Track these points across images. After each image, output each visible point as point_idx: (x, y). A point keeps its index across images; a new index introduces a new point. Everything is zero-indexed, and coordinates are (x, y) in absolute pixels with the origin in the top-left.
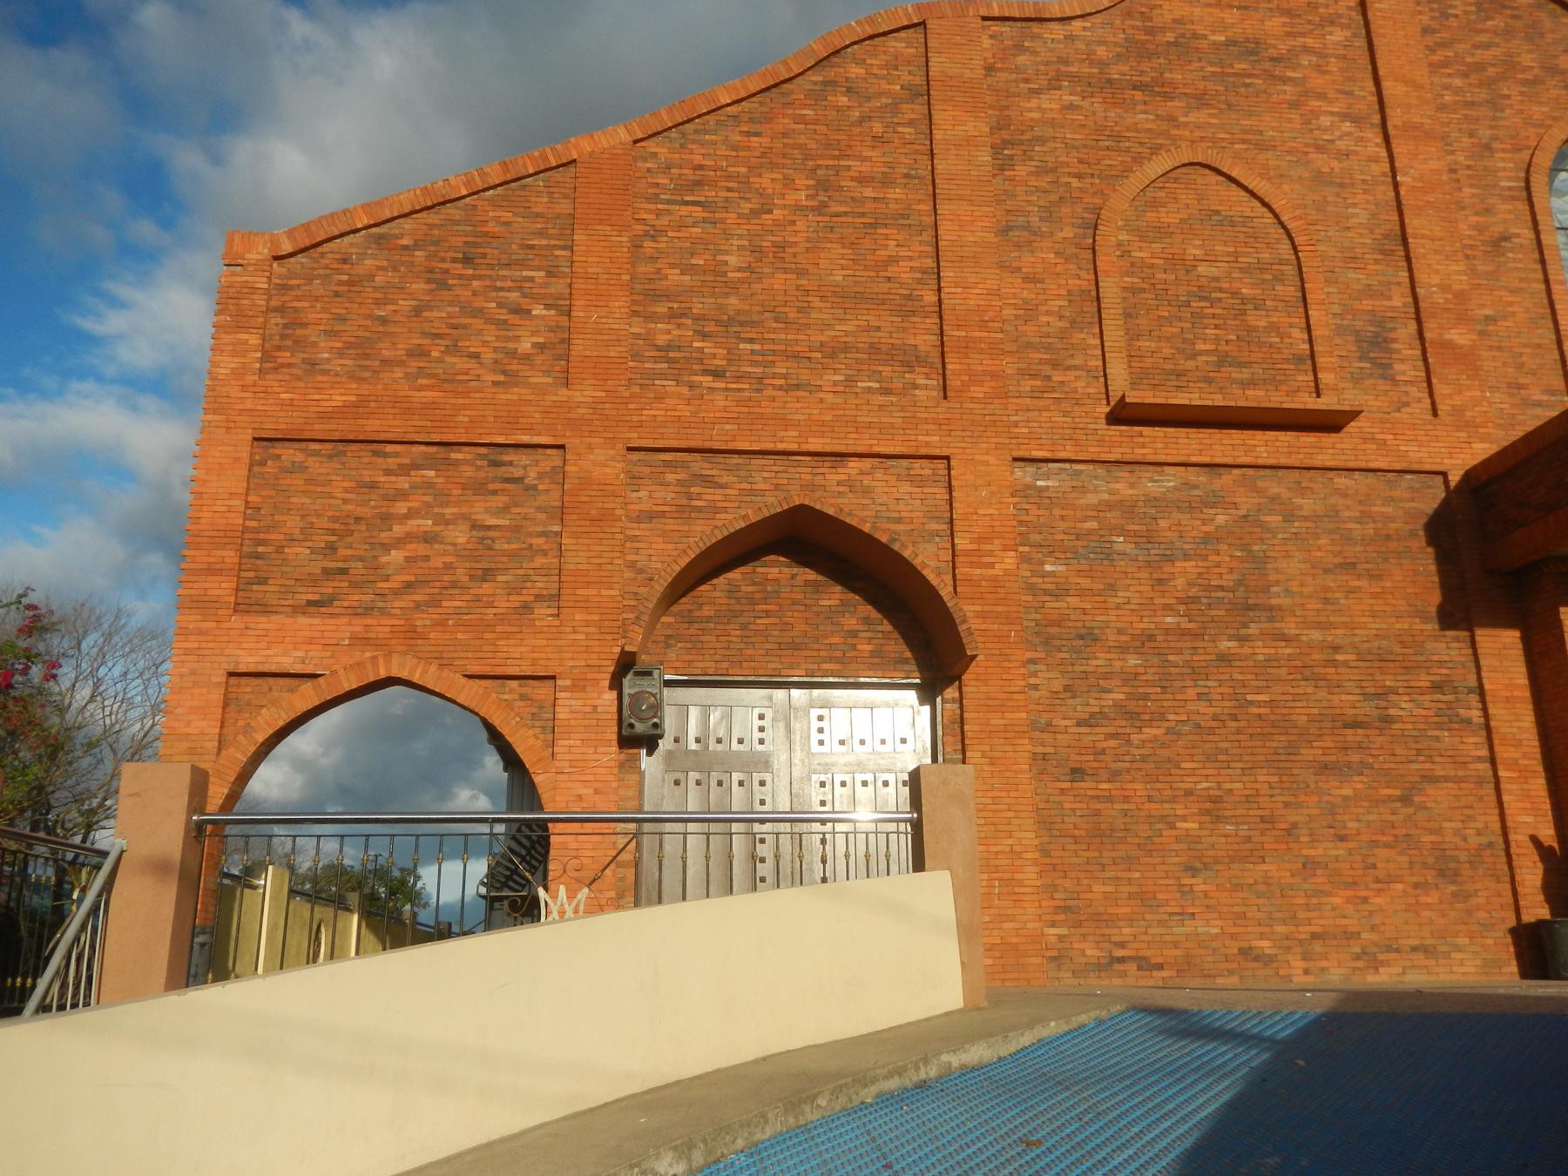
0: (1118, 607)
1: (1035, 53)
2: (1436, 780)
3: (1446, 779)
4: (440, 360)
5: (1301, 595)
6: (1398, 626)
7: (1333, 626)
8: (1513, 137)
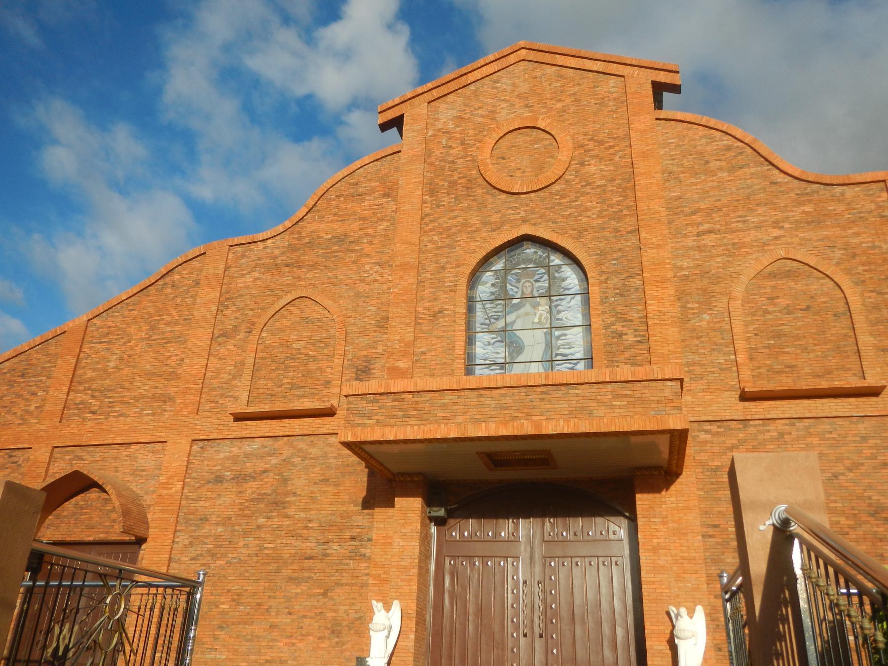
0: (220, 505)
1: (248, 257)
2: (342, 585)
3: (347, 585)
4: (4, 416)
5: (300, 495)
6: (341, 509)
7: (311, 510)
8: (457, 260)
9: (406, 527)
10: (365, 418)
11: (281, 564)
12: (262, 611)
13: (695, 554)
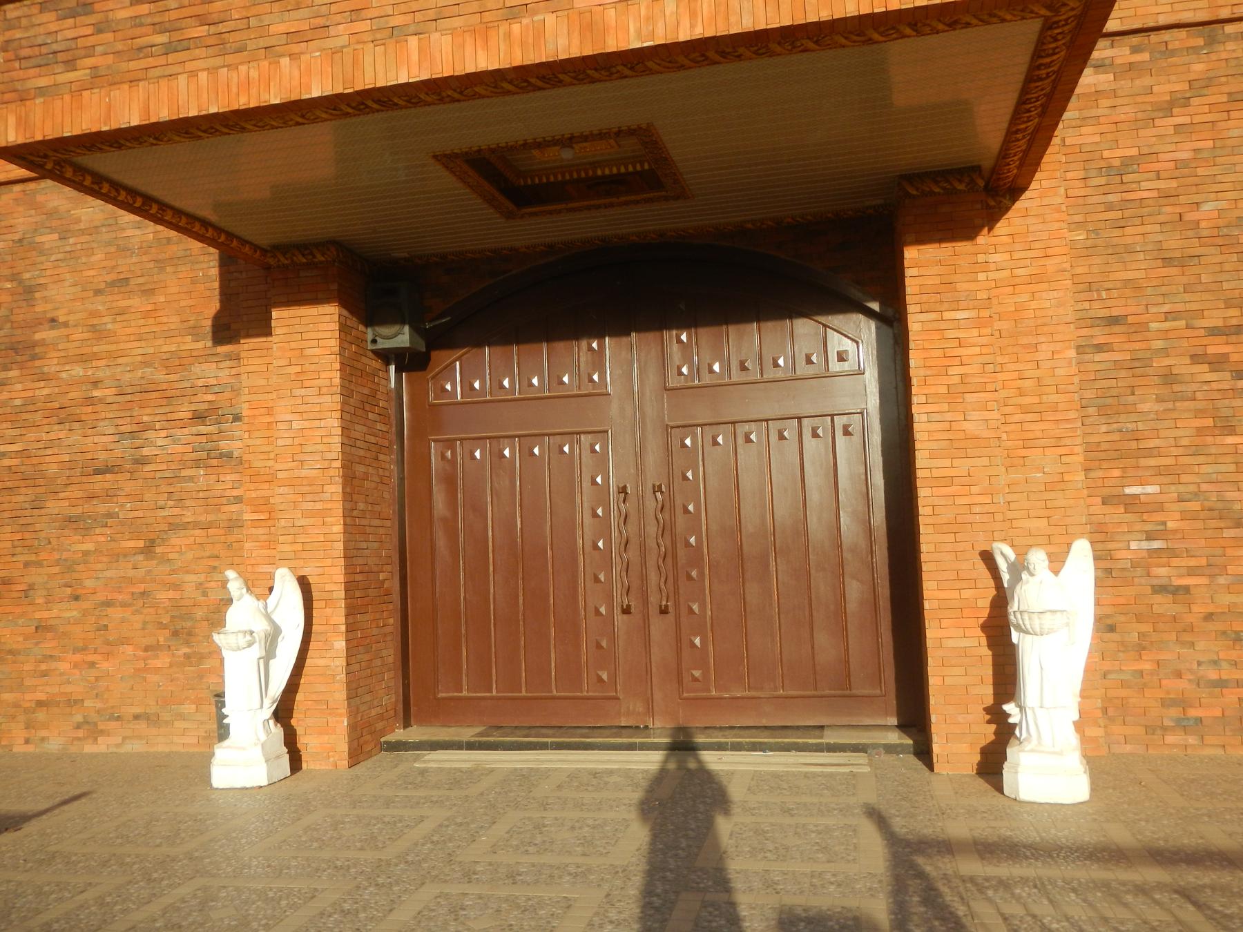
2: (185, 527)
3: (196, 525)
5: (66, 324)
6: (165, 349)
7: (95, 357)
9: (306, 384)
10: (59, 68)
11: (42, 490)
12: (15, 595)
13: (1055, 398)
